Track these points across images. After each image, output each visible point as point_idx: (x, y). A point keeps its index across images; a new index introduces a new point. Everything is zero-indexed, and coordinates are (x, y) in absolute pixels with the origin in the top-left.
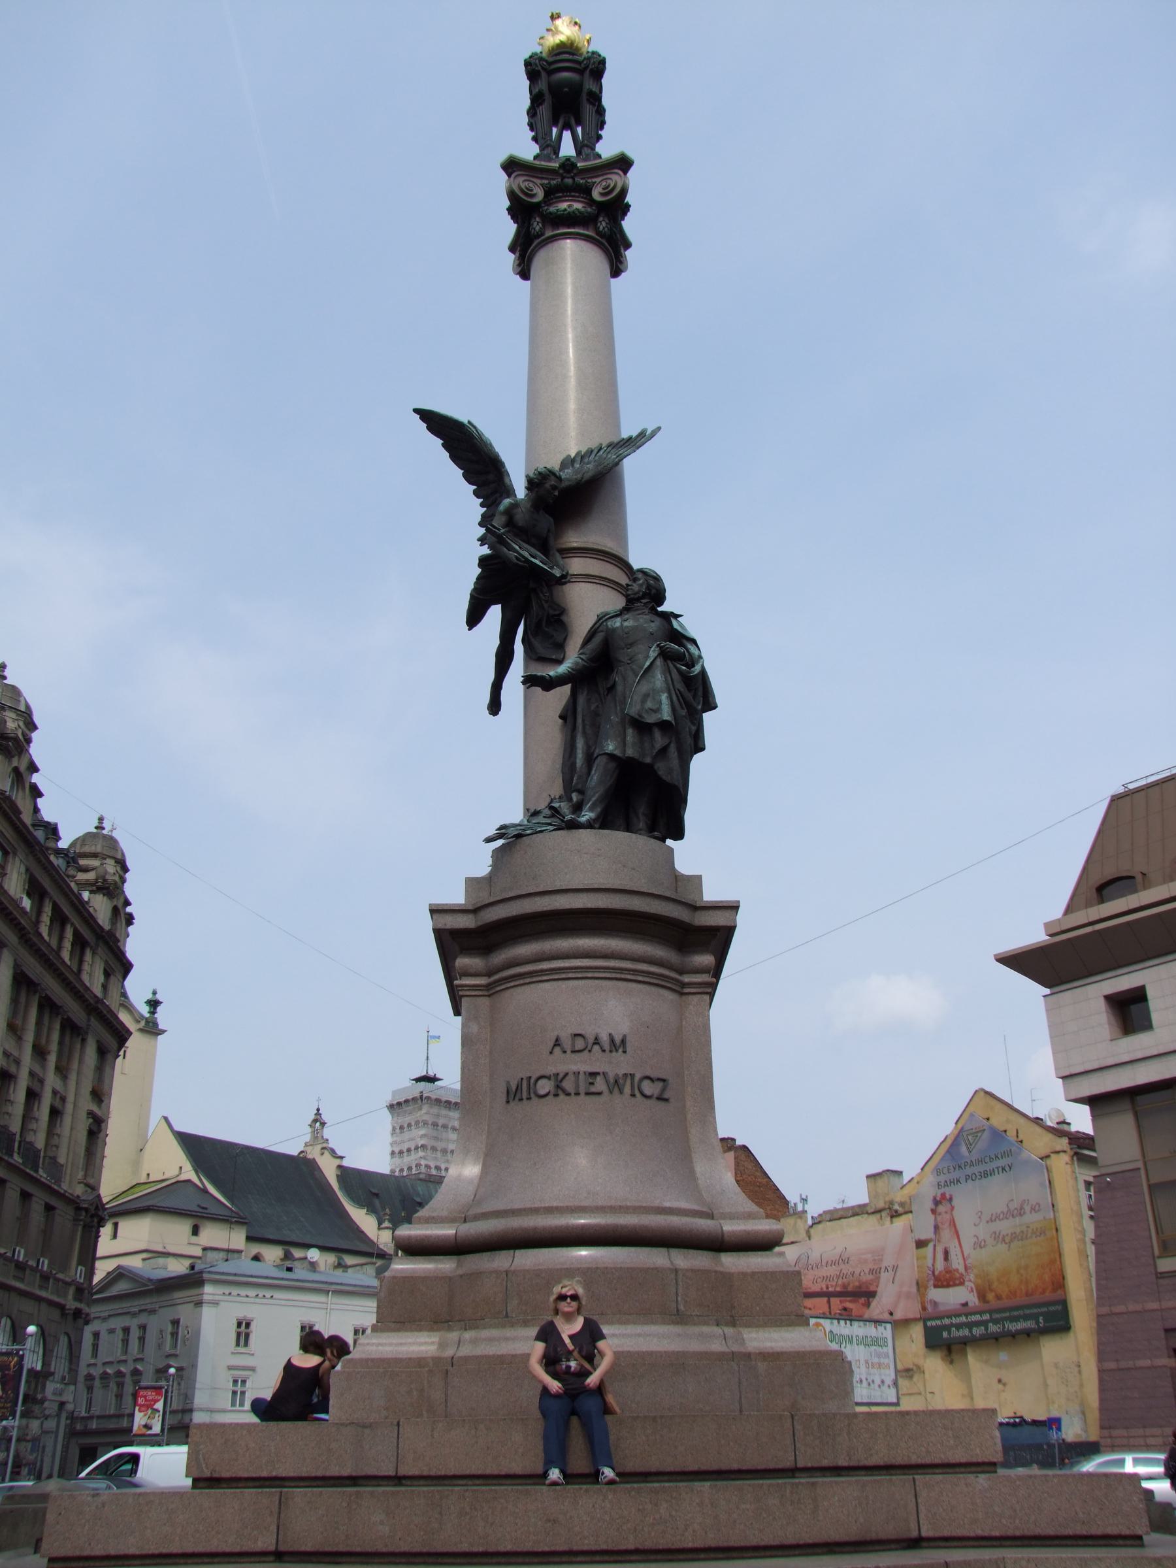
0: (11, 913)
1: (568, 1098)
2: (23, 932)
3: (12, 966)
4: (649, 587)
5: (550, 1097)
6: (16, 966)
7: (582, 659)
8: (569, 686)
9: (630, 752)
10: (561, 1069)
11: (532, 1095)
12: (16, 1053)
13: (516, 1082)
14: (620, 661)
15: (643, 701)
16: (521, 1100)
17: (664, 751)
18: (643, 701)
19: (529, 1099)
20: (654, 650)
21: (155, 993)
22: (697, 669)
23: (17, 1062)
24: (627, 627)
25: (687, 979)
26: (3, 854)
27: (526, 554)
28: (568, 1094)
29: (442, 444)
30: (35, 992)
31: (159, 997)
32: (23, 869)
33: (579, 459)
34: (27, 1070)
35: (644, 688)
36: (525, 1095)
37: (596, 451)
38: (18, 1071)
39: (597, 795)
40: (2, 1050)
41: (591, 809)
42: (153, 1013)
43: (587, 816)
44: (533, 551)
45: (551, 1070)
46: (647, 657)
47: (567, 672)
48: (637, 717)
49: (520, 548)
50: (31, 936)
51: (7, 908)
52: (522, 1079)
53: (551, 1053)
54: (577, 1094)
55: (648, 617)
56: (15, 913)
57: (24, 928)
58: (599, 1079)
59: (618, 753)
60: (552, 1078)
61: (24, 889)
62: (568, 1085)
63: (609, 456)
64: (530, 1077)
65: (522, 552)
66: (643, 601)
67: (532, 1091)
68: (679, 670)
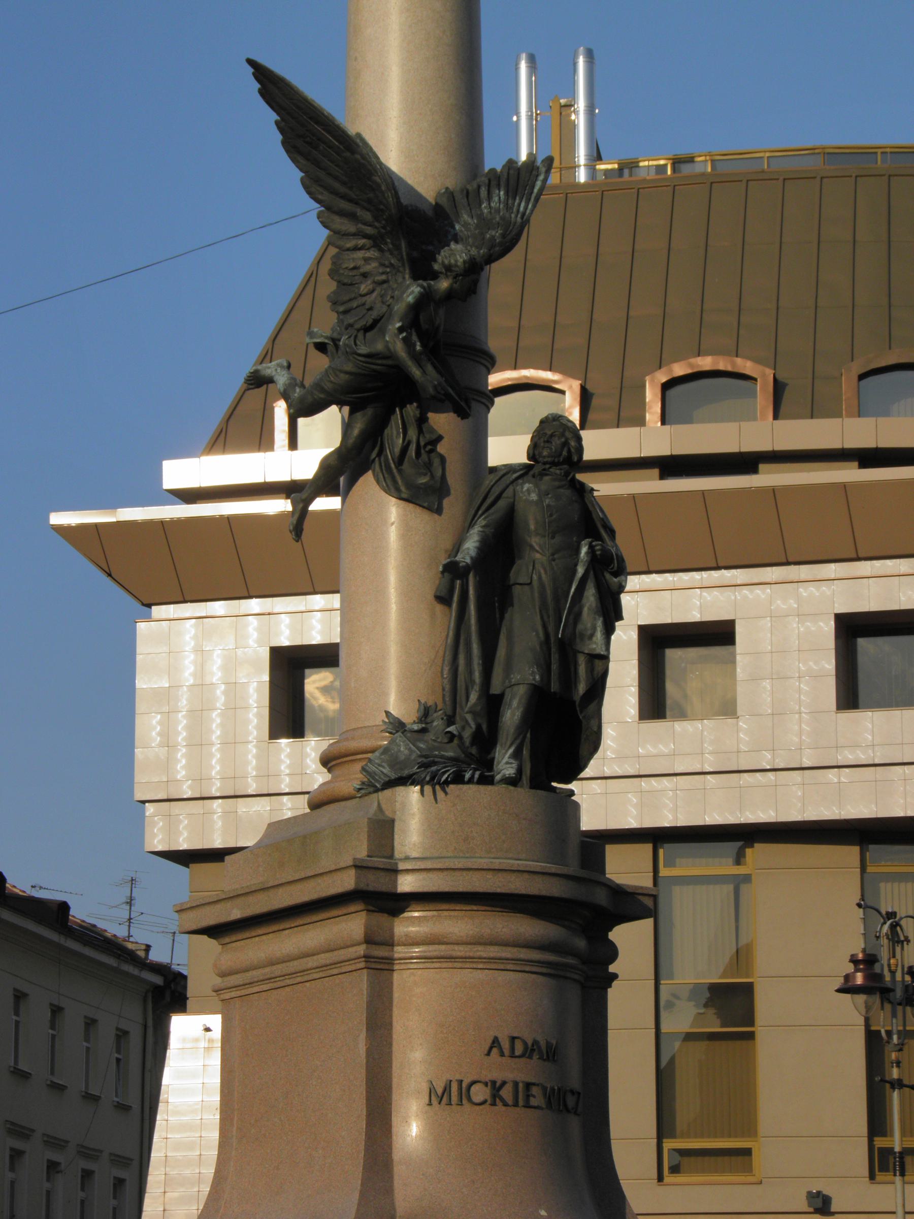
1: (504, 1108)
5: (487, 1106)
10: (497, 1075)
11: (465, 1101)
13: (442, 1085)
14: (531, 547)
16: (450, 1104)
19: (460, 1103)
28: (506, 1104)
29: (277, 123)
36: (455, 1098)
37: (483, 192)
45: (488, 1076)
52: (451, 1081)
53: (488, 1054)
54: (516, 1104)
58: (535, 1090)
60: (489, 1084)
62: (506, 1093)
64: (460, 1082)
67: (464, 1097)
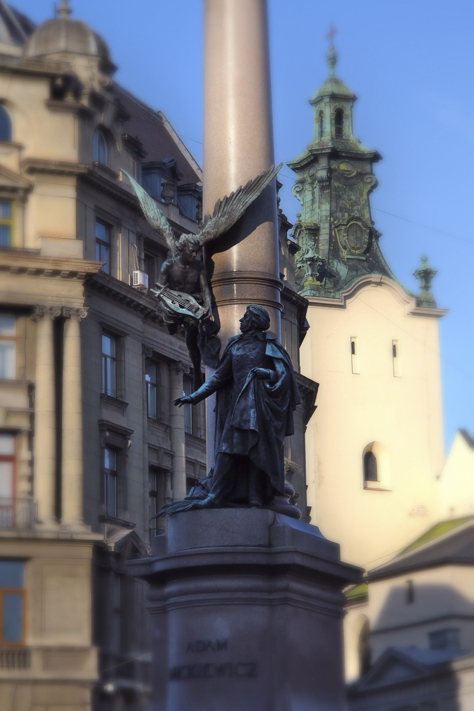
0: (125, 297)
2: (146, 312)
3: (140, 353)
4: (253, 322)
6: (145, 349)
7: (216, 377)
8: (215, 393)
9: (236, 451)
12: (166, 446)
15: (242, 415)
17: (255, 447)
18: (242, 415)
20: (249, 376)
21: (425, 260)
22: (279, 384)
23: (172, 455)
24: (238, 355)
25: (272, 597)
26: (106, 228)
27: (176, 307)
30: (178, 371)
31: (432, 265)
32: (133, 238)
33: (223, 206)
34: (184, 460)
35: (243, 404)
38: (172, 464)
39: (217, 481)
40: (146, 446)
41: (213, 492)
42: (426, 287)
43: (211, 496)
44: (186, 296)
46: (246, 380)
47: (205, 390)
48: (237, 426)
49: (172, 302)
50: (157, 313)
51: (119, 293)
55: (251, 346)
56: (129, 296)
57: (146, 308)
59: (227, 451)
61: (140, 259)
63: (238, 206)
65: (172, 306)
66: (250, 333)
68: (265, 387)
